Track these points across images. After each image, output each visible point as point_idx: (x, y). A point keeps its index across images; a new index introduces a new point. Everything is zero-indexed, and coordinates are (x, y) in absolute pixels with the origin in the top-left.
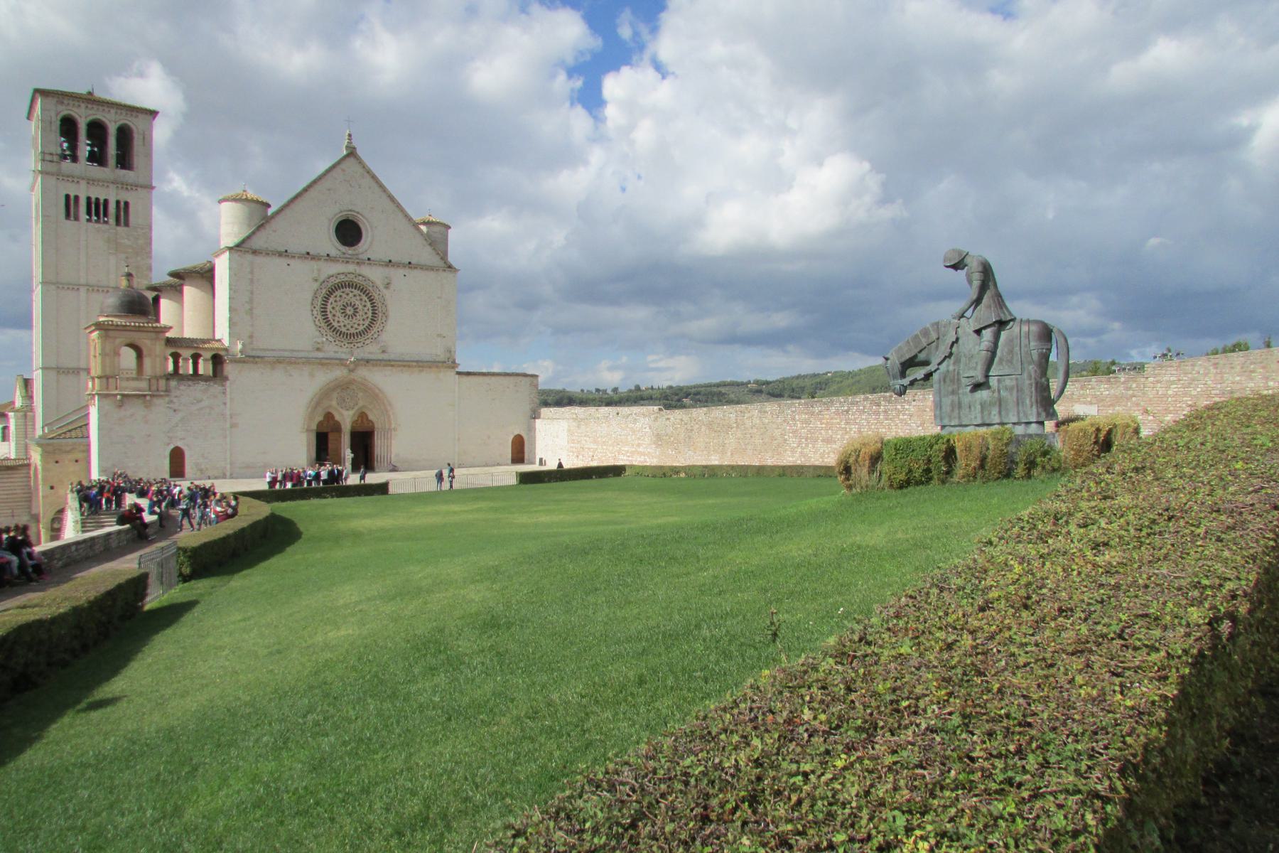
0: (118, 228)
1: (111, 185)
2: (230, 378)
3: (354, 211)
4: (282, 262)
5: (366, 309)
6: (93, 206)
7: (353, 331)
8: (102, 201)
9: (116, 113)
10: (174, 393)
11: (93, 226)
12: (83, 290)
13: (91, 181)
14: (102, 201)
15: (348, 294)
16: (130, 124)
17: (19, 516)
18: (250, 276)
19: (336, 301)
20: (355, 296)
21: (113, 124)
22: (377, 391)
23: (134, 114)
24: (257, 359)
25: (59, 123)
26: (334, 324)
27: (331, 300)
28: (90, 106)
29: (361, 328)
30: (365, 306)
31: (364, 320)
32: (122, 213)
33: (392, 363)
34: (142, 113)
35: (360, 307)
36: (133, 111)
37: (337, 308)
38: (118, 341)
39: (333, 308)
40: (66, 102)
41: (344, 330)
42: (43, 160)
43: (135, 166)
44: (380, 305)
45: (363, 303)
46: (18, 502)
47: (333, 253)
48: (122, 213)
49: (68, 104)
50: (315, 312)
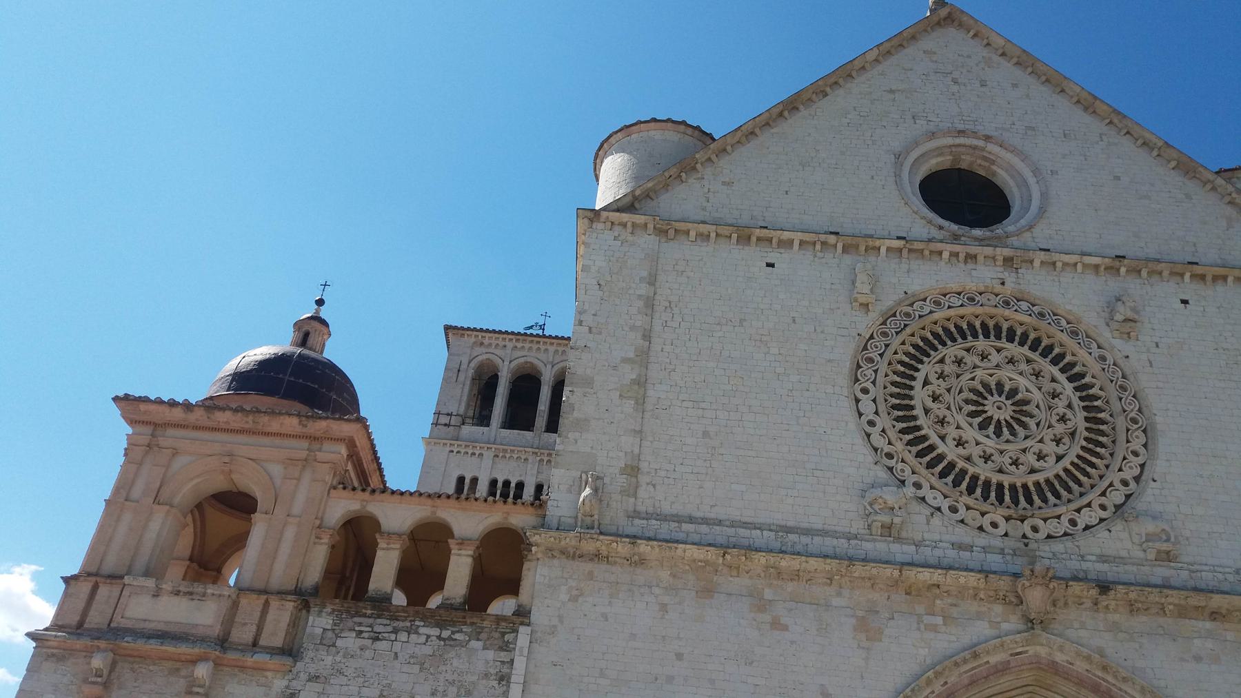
1: (531, 459)
3: (975, 134)
4: (754, 256)
5: (1060, 405)
7: (1018, 477)
9: (556, 351)
10: (316, 660)
15: (984, 357)
18: (644, 290)
19: (941, 376)
20: (1011, 361)
21: (549, 366)
24: (643, 547)
25: (471, 372)
26: (942, 448)
27: (927, 369)
28: (519, 345)
30: (1055, 395)
31: (1058, 441)
33: (1217, 601)
35: (1037, 396)
39: (935, 398)
40: (486, 341)
41: (984, 471)
42: (435, 424)
44: (1112, 392)
45: (1048, 386)
49: (490, 345)
50: (867, 406)
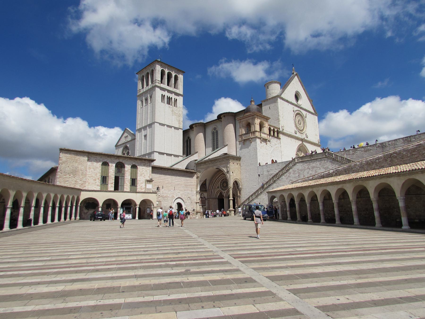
0: (174, 107)
2: (281, 138)
3: (298, 92)
6: (168, 99)
7: (301, 129)
8: (170, 98)
11: (168, 105)
12: (166, 126)
13: (169, 91)
14: (170, 98)
16: (177, 75)
17: (193, 191)
22: (307, 150)
23: (179, 72)
27: (296, 118)
28: (168, 68)
29: (302, 129)
32: (175, 102)
34: (181, 72)
36: (179, 71)
37: (297, 121)
38: (259, 120)
40: (163, 65)
43: (179, 88)
46: (193, 186)
47: (296, 104)
48: (175, 102)
49: (163, 66)
